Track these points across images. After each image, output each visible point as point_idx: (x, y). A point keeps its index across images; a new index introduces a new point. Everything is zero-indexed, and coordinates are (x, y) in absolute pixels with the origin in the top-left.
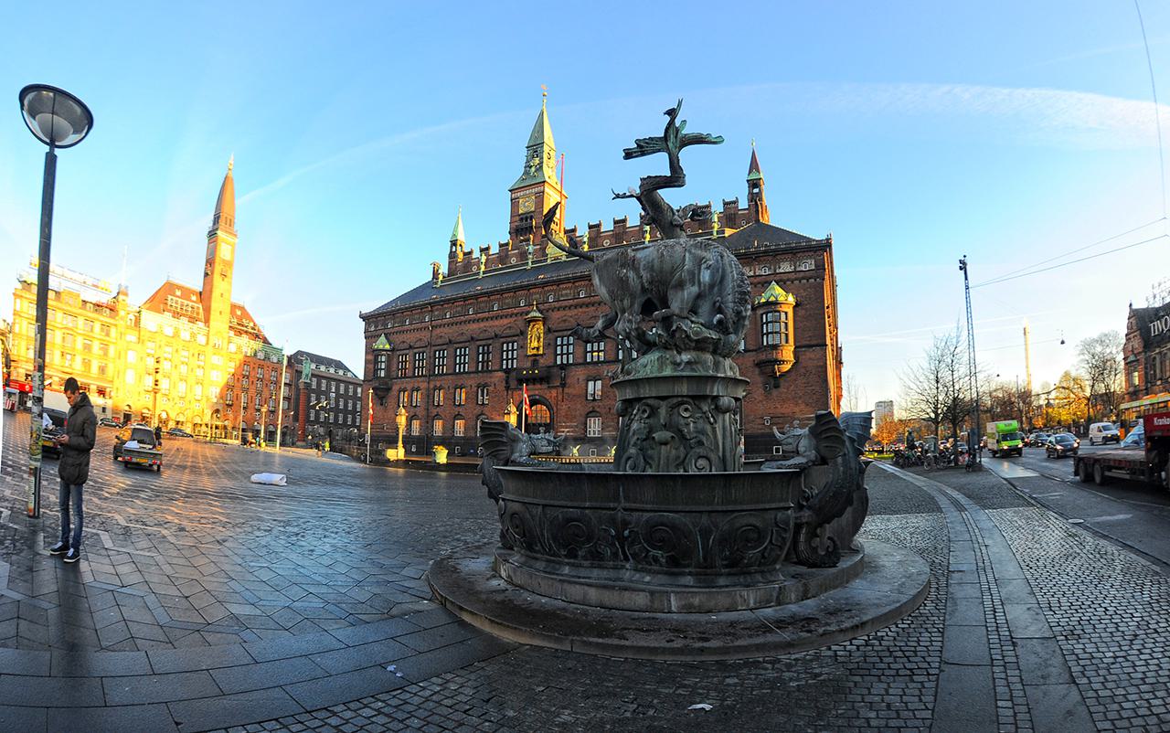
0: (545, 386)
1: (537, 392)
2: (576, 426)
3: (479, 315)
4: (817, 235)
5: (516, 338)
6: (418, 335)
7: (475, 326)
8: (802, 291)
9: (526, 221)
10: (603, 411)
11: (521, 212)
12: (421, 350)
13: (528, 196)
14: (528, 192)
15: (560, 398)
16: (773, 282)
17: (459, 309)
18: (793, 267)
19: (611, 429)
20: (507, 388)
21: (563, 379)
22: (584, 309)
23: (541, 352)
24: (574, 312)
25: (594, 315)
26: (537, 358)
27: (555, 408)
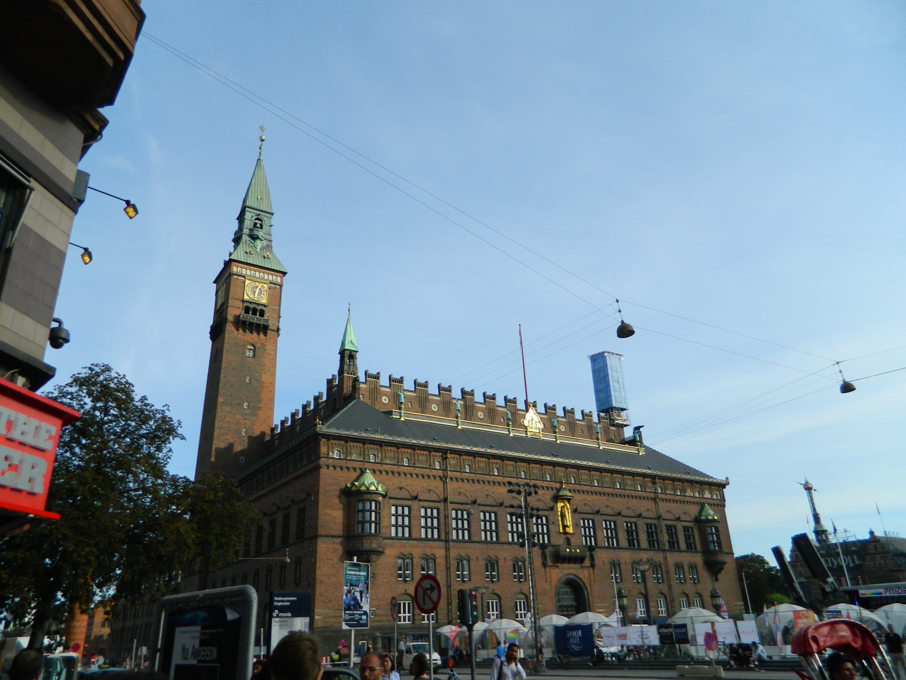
0: (578, 566)
1: (572, 571)
3: (506, 478)
4: (719, 477)
6: (426, 483)
9: (254, 313)
11: (246, 297)
12: (432, 504)
13: (261, 281)
14: (257, 274)
20: (544, 565)
21: (592, 558)
22: (598, 497)
24: (591, 498)
26: (568, 536)
27: (589, 589)
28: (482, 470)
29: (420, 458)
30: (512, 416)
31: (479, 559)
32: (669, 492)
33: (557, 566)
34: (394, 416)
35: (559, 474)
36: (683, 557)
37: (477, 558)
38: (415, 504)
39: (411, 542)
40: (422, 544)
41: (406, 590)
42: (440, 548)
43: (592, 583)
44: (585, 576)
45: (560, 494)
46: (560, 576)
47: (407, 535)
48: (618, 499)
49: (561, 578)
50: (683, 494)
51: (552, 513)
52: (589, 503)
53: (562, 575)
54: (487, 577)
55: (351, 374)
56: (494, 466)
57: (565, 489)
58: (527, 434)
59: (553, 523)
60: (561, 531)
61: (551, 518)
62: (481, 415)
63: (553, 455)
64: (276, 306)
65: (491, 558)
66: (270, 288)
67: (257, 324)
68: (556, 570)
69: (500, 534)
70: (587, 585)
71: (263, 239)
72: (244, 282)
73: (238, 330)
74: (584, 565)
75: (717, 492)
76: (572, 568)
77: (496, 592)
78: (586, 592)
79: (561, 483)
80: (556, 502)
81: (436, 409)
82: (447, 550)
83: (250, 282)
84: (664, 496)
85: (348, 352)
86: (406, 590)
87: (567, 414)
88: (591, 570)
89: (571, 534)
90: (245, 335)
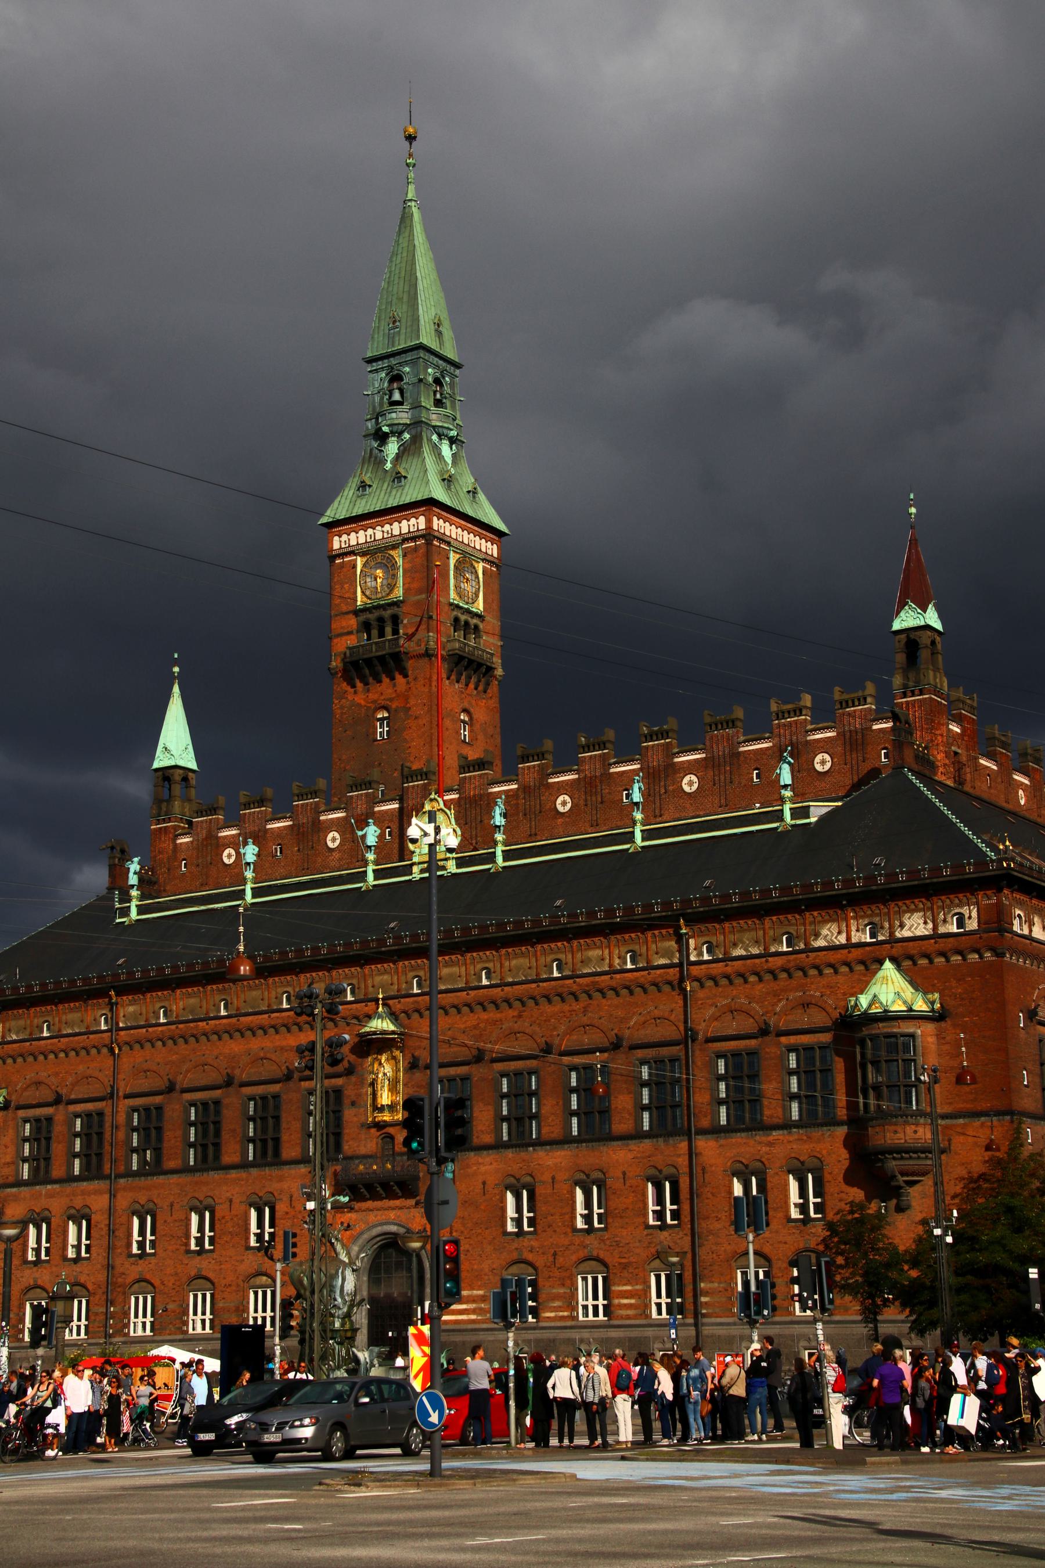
0: (412, 1202)
2: (483, 1299)
3: (242, 1019)
7: (234, 1047)
8: (954, 983)
10: (540, 1262)
12: (90, 1106)
16: (888, 964)
17: (192, 1001)
18: (930, 925)
19: (557, 1304)
22: (492, 1014)
28: (192, 1012)
31: (176, 1207)
32: (739, 952)
34: (118, 921)
36: (770, 1144)
37: (172, 1205)
38: (59, 1114)
39: (49, 1187)
40: (69, 1188)
41: (35, 1280)
42: (101, 1194)
48: (557, 1007)
50: (802, 946)
51: (353, 1078)
55: (164, 821)
57: (380, 1017)
61: (349, 1093)
64: (420, 591)
66: (404, 556)
67: (379, 658)
71: (400, 427)
72: (355, 567)
73: (354, 686)
75: (965, 910)
77: (204, 1273)
82: (112, 1195)
83: (365, 559)
84: (718, 968)
85: (161, 773)
86: (35, 1280)
90: (368, 691)
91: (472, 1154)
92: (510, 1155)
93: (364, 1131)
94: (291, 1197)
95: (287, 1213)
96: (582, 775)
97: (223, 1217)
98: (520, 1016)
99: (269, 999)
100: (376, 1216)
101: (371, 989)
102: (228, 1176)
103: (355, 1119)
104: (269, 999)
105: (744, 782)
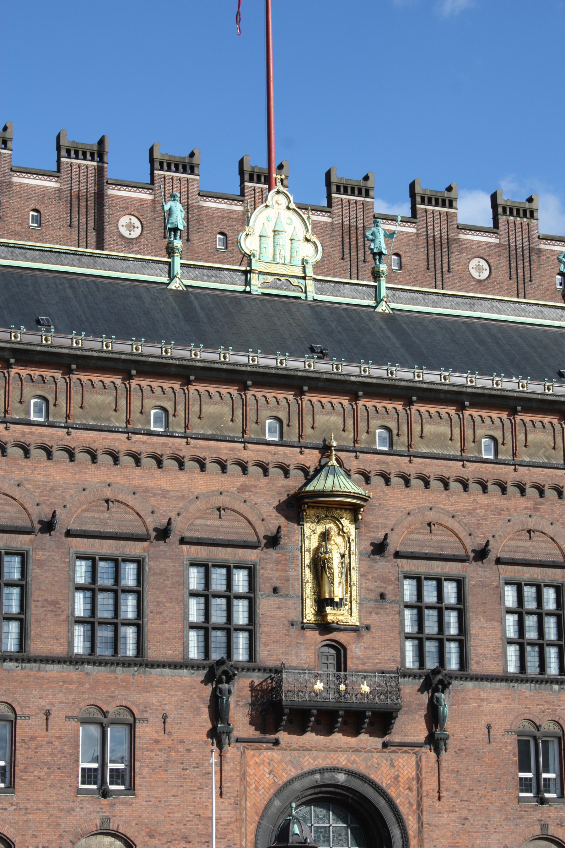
0: (377, 742)
1: (342, 760)
5: (251, 556)
15: (430, 784)
23: (354, 620)
25: (531, 524)
29: (429, 428)
30: (187, 219)
33: (276, 743)
35: (321, 419)
43: (426, 802)
44: (397, 778)
45: (310, 488)
46: (285, 778)
47: (130, 650)
49: (291, 782)
52: (450, 523)
53: (294, 773)
54: (525, 785)
56: (28, 390)
58: (247, 283)
59: (275, 590)
60: (310, 615)
62: (130, 227)
63: (312, 350)
65: (538, 728)
68: (275, 754)
69: (33, 630)
70: (403, 809)
74: (395, 737)
76: (338, 749)
78: (396, 832)
79: (325, 449)
80: (299, 520)
81: (136, 233)
87: (502, 219)
88: (428, 755)
89: (355, 629)
91: (470, 685)
92: (528, 693)
93: (294, 632)
94: (165, 717)
95: (157, 742)
96: (338, 221)
97: (33, 738)
98: (536, 509)
99: (128, 411)
100: (315, 759)
101: (308, 431)
102: (42, 674)
103: (280, 613)
104: (128, 411)
105: (546, 285)
